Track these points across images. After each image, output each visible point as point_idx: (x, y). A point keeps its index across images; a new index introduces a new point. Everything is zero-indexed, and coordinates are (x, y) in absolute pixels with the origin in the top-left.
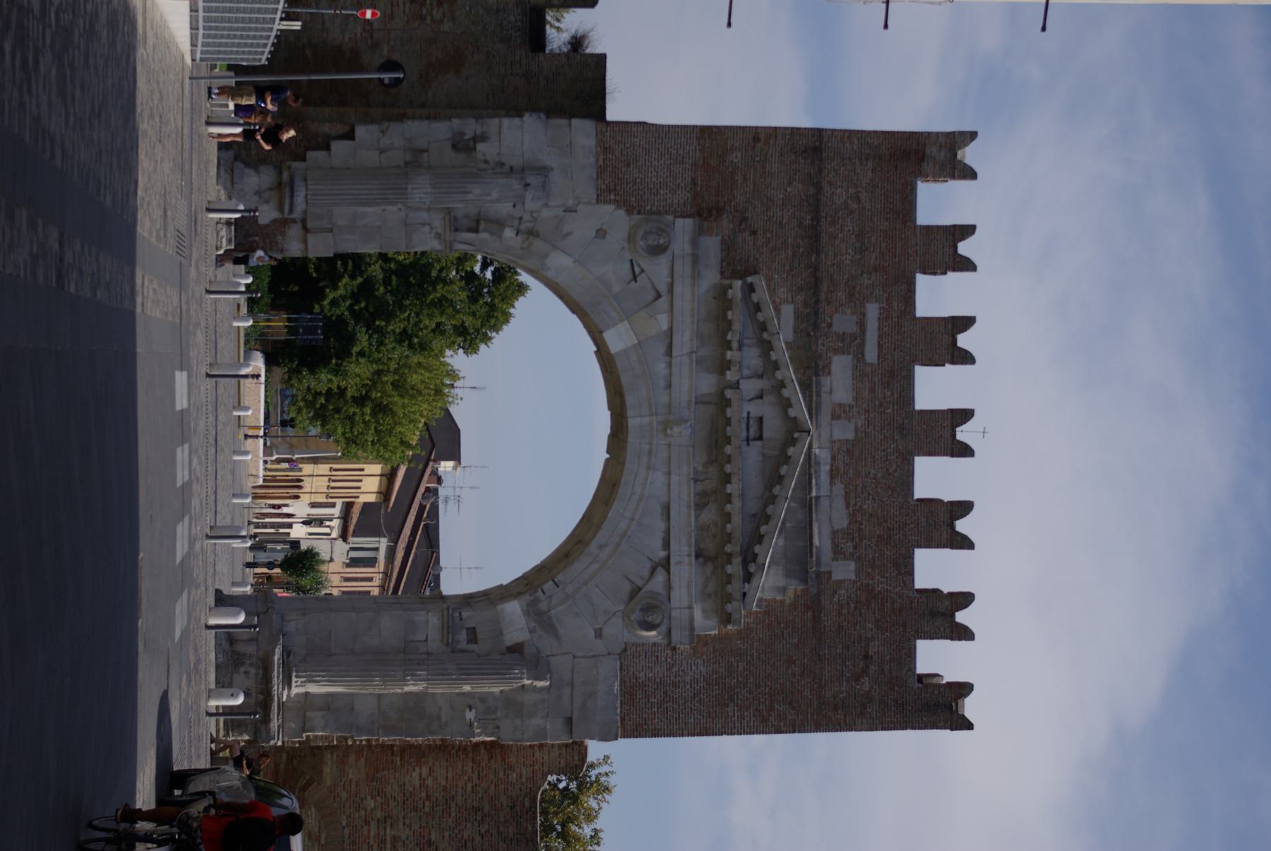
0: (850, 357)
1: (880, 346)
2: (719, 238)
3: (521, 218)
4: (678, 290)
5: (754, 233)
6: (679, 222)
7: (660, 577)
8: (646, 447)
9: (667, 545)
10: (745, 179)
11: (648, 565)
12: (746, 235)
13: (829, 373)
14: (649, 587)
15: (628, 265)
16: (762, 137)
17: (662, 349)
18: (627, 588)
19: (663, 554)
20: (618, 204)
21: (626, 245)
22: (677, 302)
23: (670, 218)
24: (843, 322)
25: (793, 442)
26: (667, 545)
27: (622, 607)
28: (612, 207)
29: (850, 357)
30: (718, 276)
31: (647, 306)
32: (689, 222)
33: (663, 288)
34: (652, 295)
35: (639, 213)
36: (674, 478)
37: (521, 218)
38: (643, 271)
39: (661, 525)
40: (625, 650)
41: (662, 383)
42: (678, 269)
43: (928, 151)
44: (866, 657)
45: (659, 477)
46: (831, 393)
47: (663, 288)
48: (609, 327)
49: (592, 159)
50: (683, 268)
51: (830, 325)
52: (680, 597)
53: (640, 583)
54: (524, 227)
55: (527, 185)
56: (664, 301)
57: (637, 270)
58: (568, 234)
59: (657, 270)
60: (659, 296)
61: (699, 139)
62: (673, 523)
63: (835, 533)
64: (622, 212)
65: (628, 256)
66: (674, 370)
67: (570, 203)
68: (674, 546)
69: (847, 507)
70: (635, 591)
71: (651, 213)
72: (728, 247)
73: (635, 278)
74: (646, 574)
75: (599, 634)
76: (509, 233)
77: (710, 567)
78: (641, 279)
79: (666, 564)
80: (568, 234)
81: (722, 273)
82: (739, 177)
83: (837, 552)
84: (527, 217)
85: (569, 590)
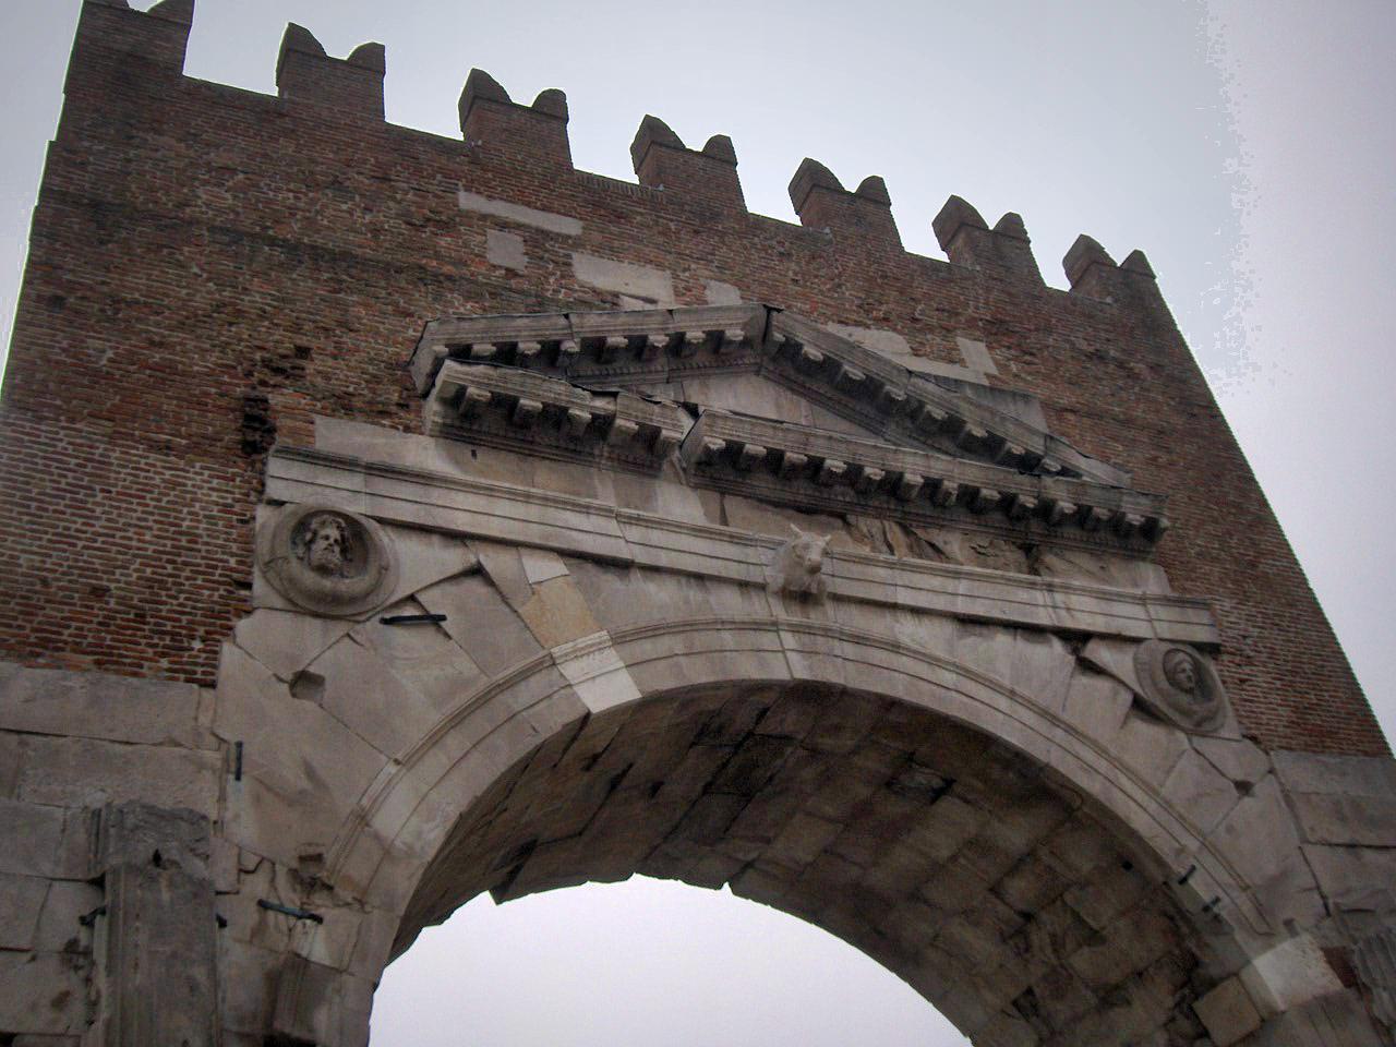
0: (575, 256)
1: (544, 209)
2: (318, 419)
3: (263, 905)
4: (461, 522)
5: (303, 352)
6: (275, 489)
7: (1099, 653)
8: (849, 650)
9: (1034, 631)
10: (161, 345)
11: (1086, 681)
12: (310, 368)
13: (616, 295)
14: (1128, 675)
15: (399, 635)
16: (49, 291)
17: (610, 581)
18: (1143, 729)
19: (1058, 646)
20: (219, 626)
21: (340, 628)
22: (493, 528)
23: (263, 514)
24: (506, 252)
25: (790, 350)
26: (1034, 631)
27: (1181, 736)
28: (228, 651)
29: (575, 256)
30: (414, 438)
31: (505, 600)
32: (275, 465)
33: (455, 558)
34: (475, 586)
35: (249, 586)
36: (904, 597)
37: (263, 905)
38: (412, 598)
39: (1002, 640)
40: (1253, 739)
41: (694, 594)
42: (407, 513)
43: (126, 48)
44: (1099, 357)
45: (908, 630)
46: (652, 301)
47: (455, 558)
48: (575, 699)
49: (76, 681)
50: (403, 503)
51: (511, 273)
52: (1130, 619)
53: (1127, 698)
54: (290, 897)
55: (157, 859)
56: (496, 562)
57: (409, 611)
58: (310, 773)
59: (416, 564)
60: (477, 571)
61: (41, 419)
62: (996, 614)
63: (916, 353)
64: (243, 626)
65: (373, 625)
66: (664, 560)
67: (212, 756)
68: (1043, 618)
69: (868, 327)
70: (1140, 706)
71: (246, 560)
72: (343, 405)
73: (437, 620)
74: (1102, 685)
75: (1244, 787)
76: (317, 946)
77: (1050, 559)
78: (434, 602)
79: (1076, 639)
80: (310, 773)
81: (407, 429)
82: (157, 357)
83: (951, 358)
84: (258, 886)
85: (1192, 844)
